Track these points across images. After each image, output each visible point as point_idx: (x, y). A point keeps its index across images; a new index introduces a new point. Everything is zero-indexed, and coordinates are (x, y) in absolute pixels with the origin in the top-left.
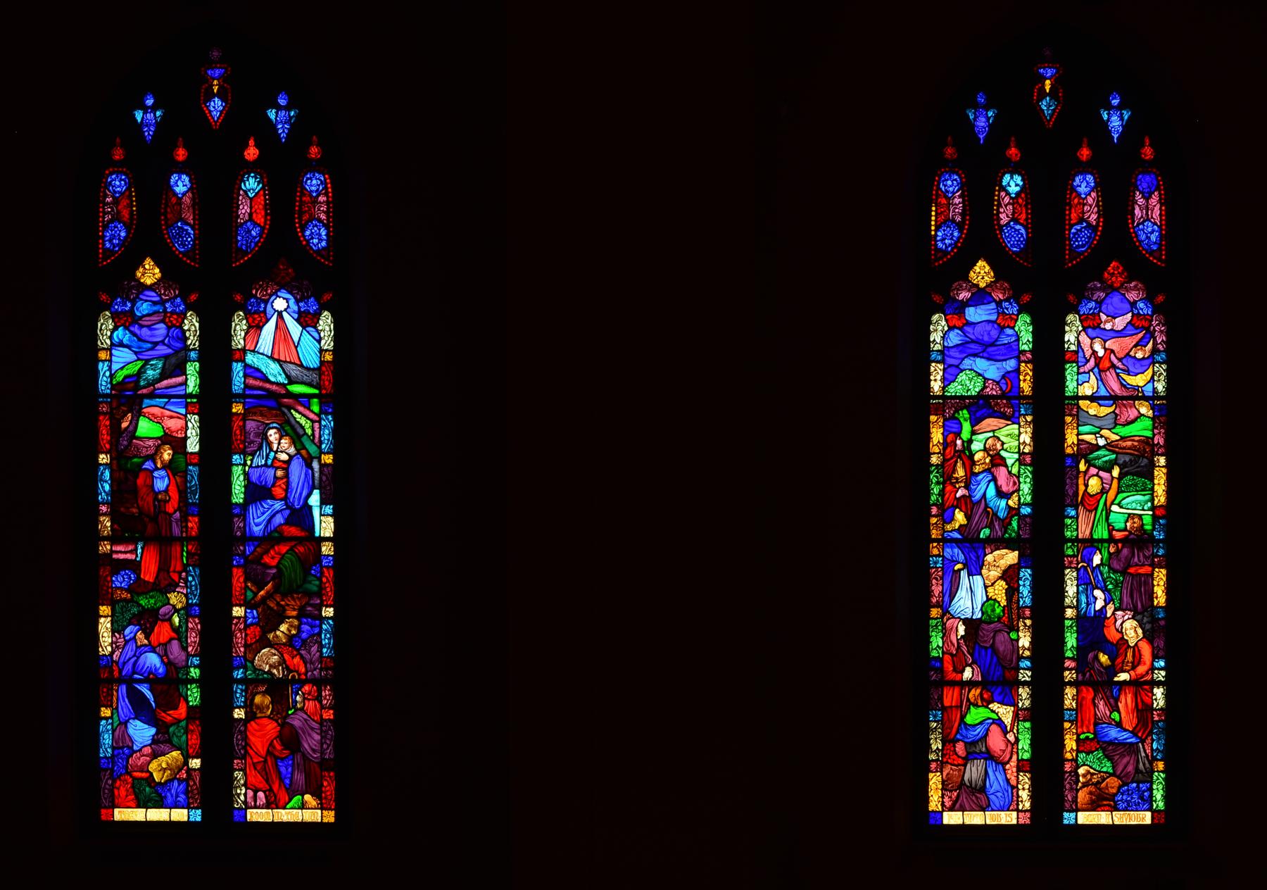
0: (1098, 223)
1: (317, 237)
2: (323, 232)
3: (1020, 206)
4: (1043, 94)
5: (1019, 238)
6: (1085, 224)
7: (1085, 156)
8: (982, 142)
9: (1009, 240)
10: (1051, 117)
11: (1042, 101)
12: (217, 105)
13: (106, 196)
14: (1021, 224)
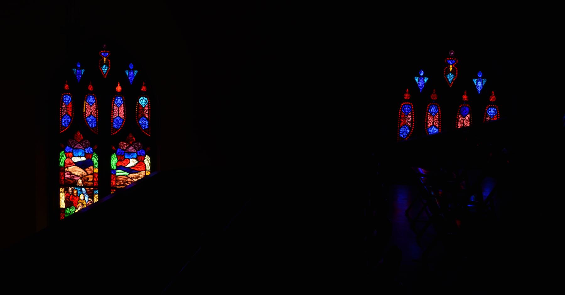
1: (144, 123)
2: (147, 122)
4: (448, 72)
10: (451, 82)
11: (448, 75)
12: (105, 69)
13: (62, 105)
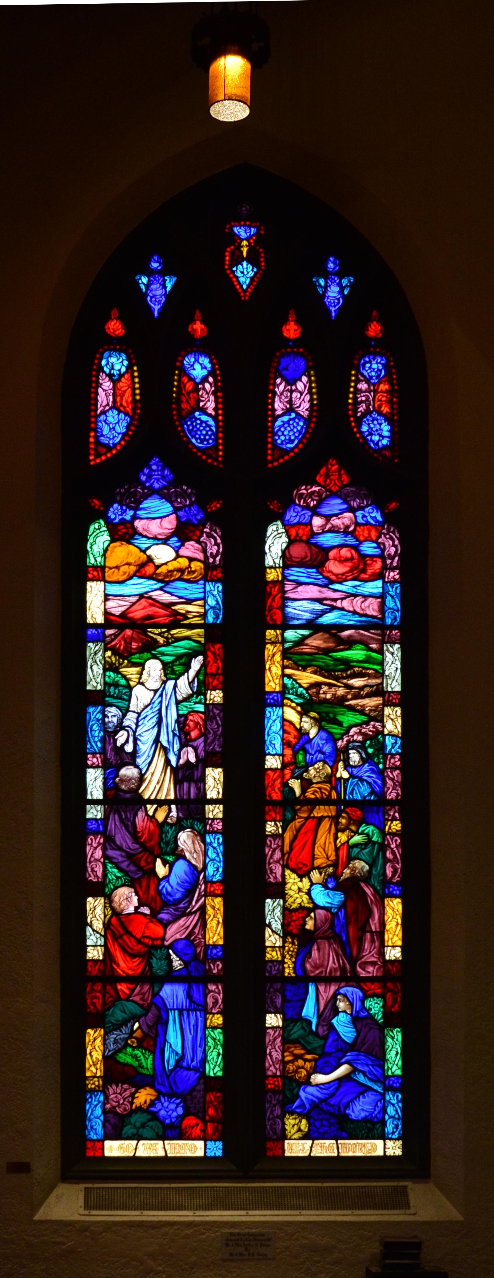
0: (310, 415)
3: (207, 393)
4: (238, 260)
5: (207, 432)
6: (293, 415)
7: (292, 332)
8: (156, 313)
9: (194, 433)
14: (209, 415)
